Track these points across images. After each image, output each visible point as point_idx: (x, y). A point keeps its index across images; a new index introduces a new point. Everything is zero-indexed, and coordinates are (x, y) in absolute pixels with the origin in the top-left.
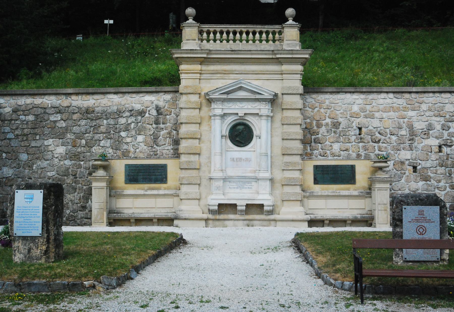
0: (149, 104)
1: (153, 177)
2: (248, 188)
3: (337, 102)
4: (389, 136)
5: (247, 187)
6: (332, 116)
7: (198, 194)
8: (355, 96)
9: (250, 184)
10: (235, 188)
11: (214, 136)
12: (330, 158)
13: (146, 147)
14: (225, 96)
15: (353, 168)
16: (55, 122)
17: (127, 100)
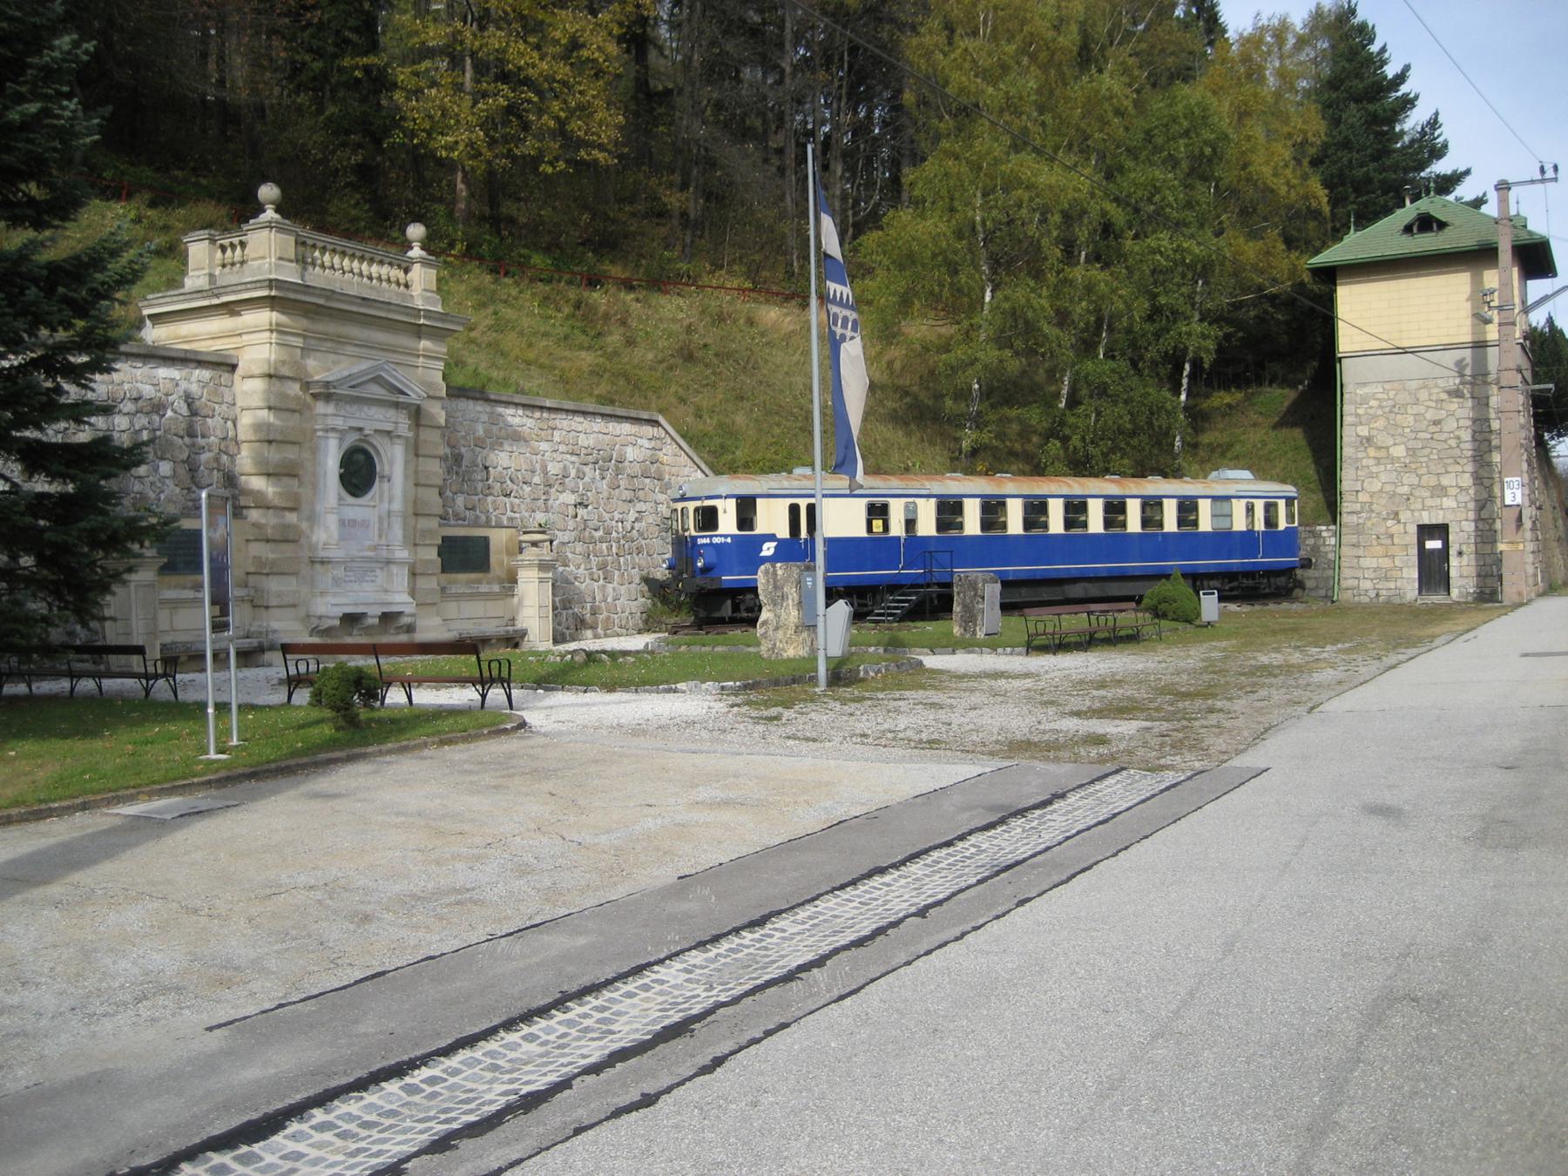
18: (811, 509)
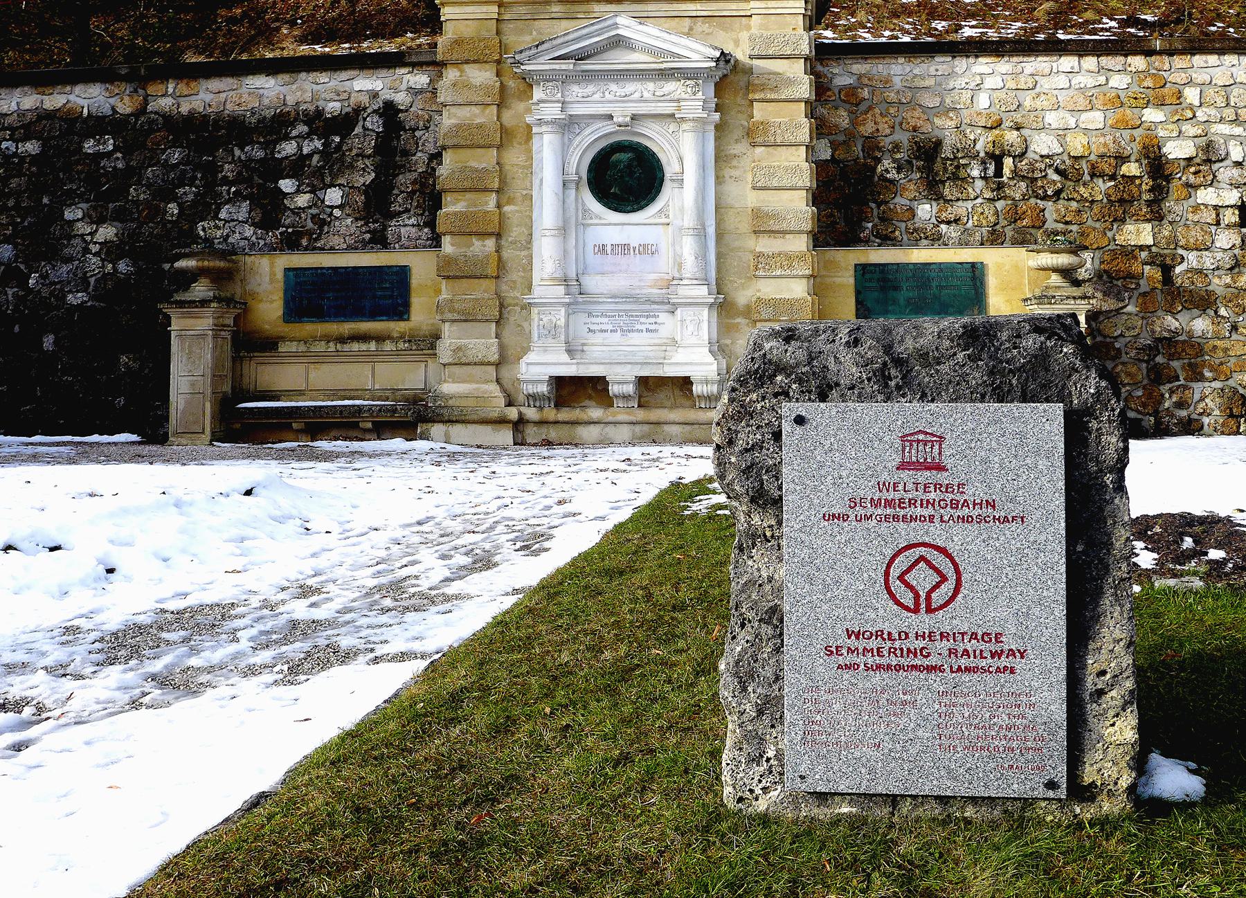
0: (364, 99)
2: (648, 331)
4: (1087, 177)
5: (643, 327)
7: (495, 349)
9: (652, 320)
10: (606, 331)
15: (975, 273)
16: (99, 156)
17: (304, 91)
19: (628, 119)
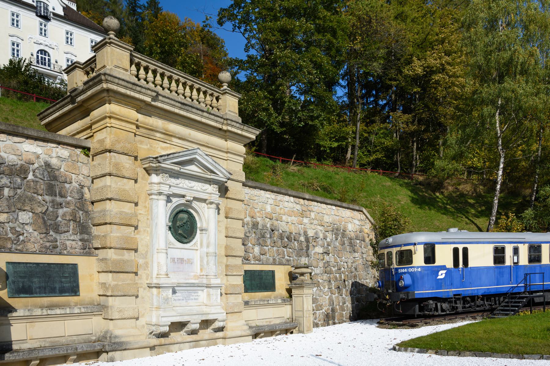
1: (57, 286)
3: (255, 198)
6: (252, 214)
8: (268, 195)
9: (196, 294)
10: (179, 300)
11: (156, 223)
12: (252, 262)
13: (36, 233)
14: (176, 168)
18: (465, 250)
19: (192, 199)
